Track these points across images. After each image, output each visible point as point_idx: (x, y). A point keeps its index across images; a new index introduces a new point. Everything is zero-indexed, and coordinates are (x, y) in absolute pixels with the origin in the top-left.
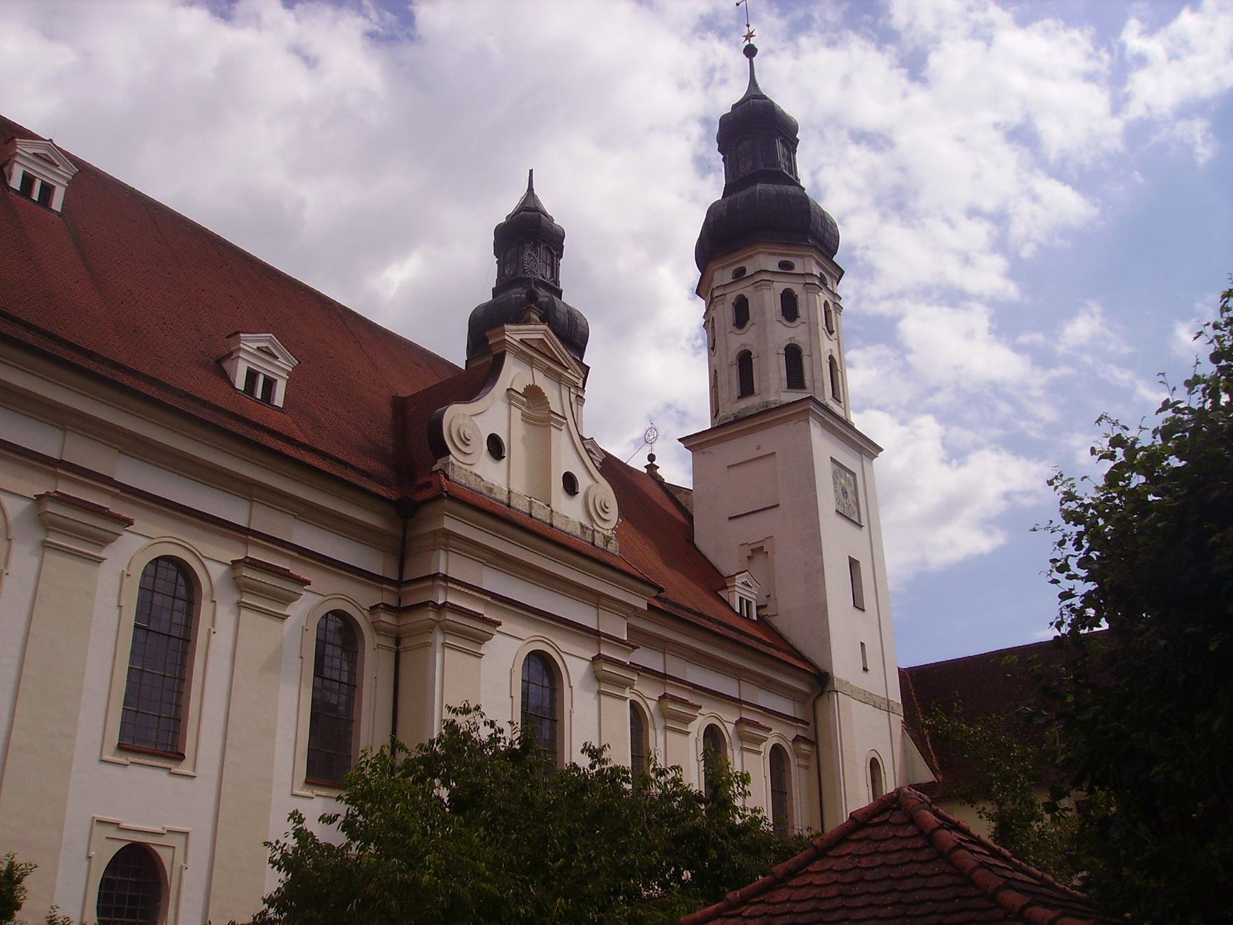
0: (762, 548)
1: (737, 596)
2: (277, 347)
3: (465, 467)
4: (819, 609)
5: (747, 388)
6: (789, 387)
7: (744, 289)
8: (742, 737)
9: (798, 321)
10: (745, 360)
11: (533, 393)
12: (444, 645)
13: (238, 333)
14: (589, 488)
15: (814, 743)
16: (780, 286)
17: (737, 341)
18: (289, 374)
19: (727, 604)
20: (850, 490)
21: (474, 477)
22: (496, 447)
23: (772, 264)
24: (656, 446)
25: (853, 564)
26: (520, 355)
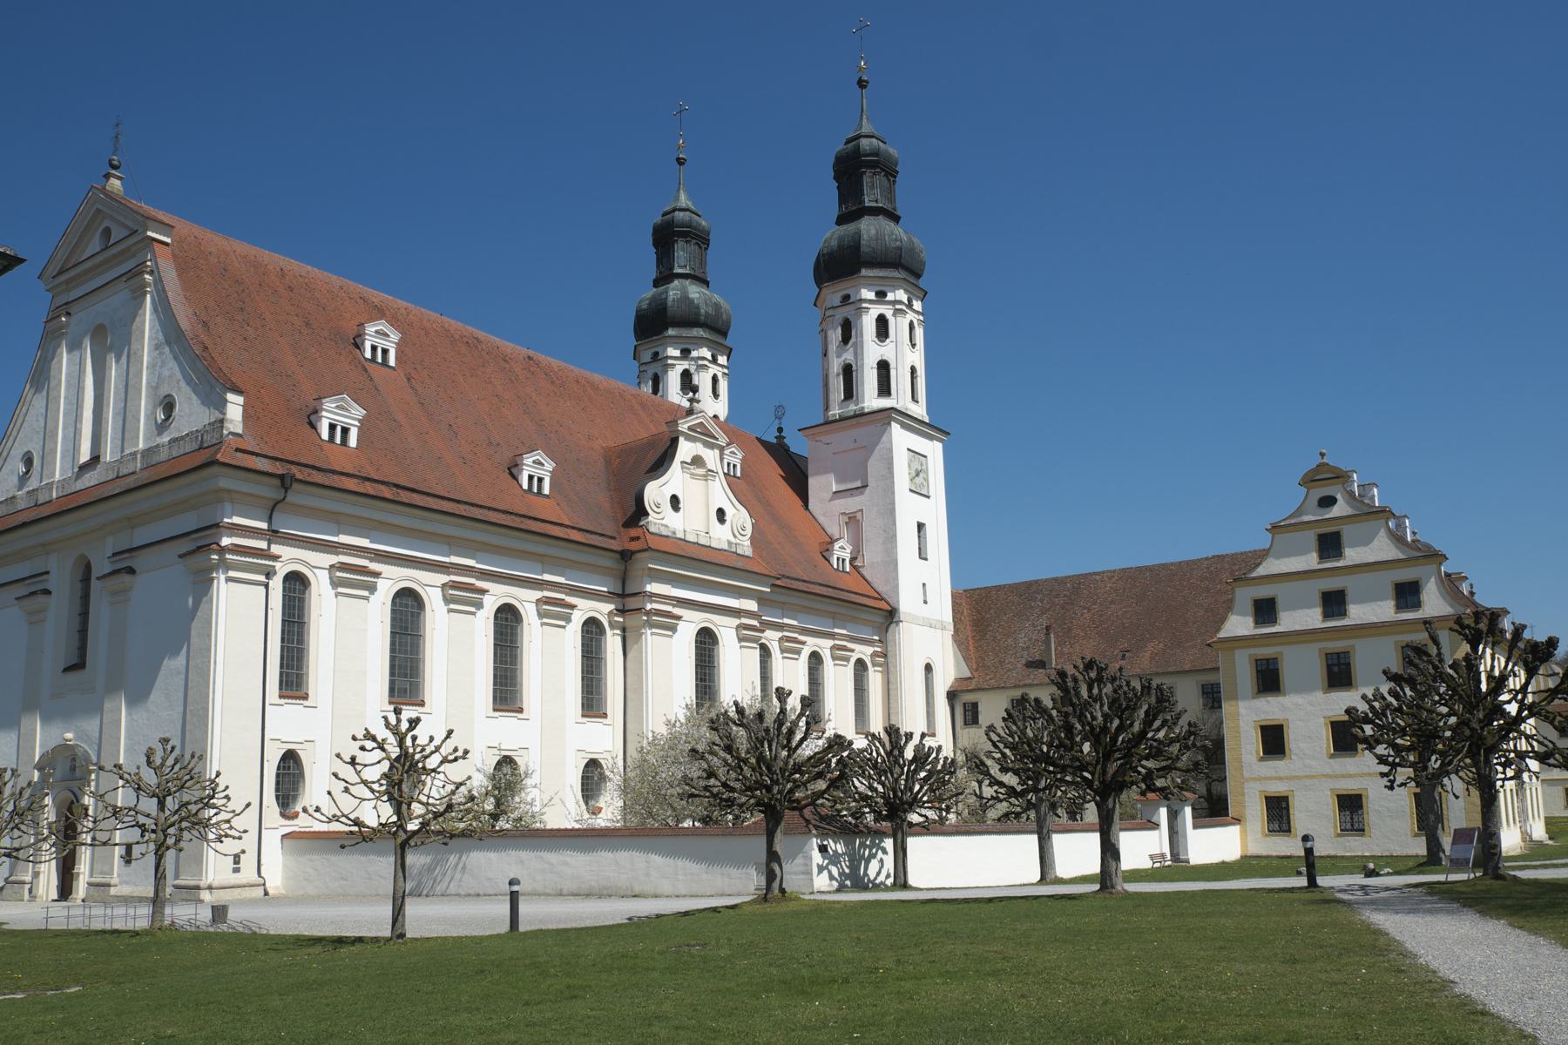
1: (835, 557)
3: (658, 521)
4: (892, 564)
6: (879, 396)
8: (834, 658)
11: (697, 461)
12: (652, 634)
13: (522, 455)
14: (734, 515)
15: (885, 656)
22: (675, 502)
24: (783, 421)
25: (920, 526)
26: (689, 438)
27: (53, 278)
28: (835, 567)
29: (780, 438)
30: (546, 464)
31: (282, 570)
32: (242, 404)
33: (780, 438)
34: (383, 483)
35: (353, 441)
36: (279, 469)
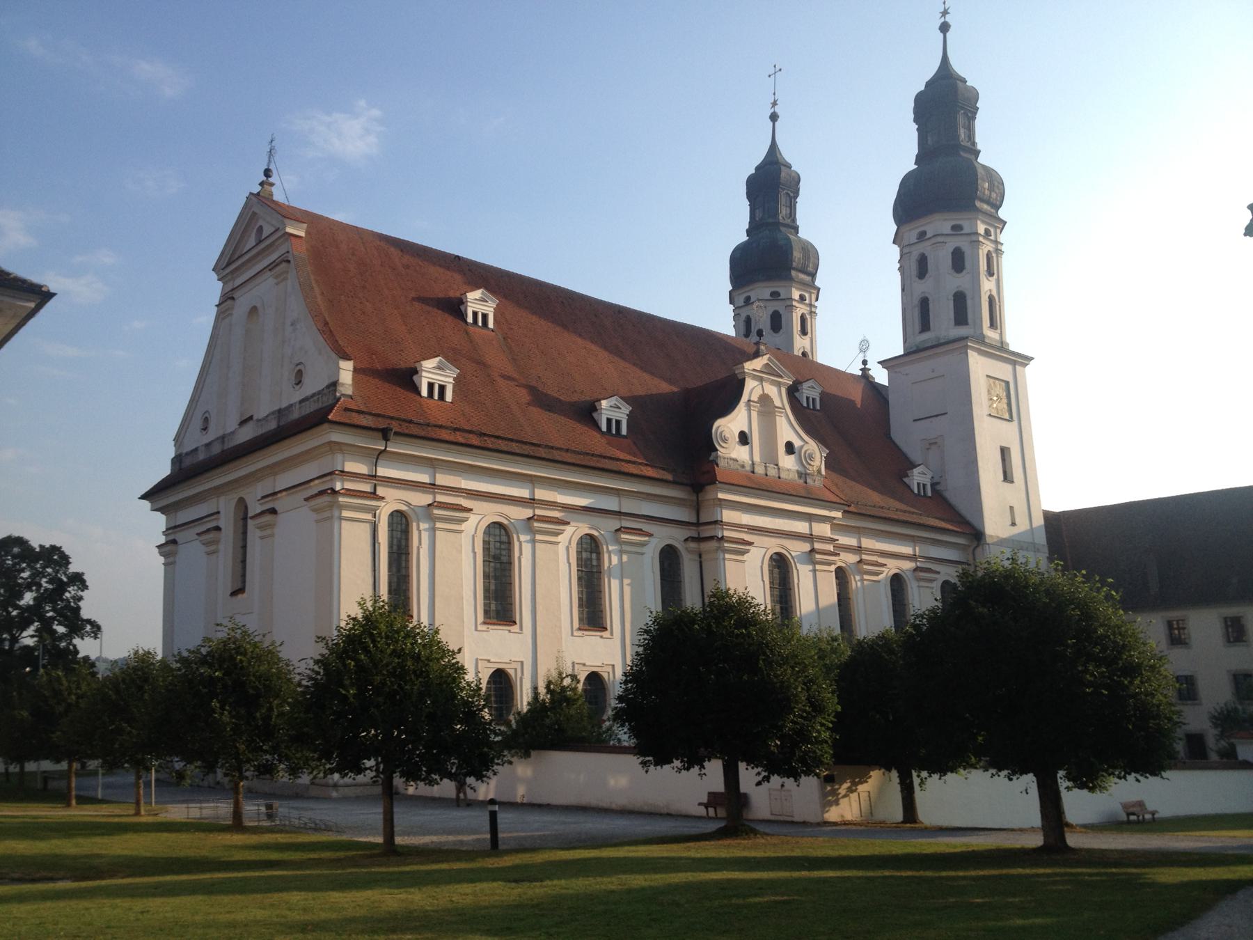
0: (936, 443)
2: (622, 404)
5: (925, 326)
7: (925, 247)
9: (964, 272)
10: (924, 304)
16: (952, 244)
17: (921, 288)
18: (627, 415)
19: (909, 487)
21: (732, 461)
23: (946, 228)
24: (867, 353)
26: (755, 378)
27: (223, 269)
28: (916, 491)
29: (865, 370)
30: (623, 408)
31: (385, 511)
32: (341, 371)
33: (865, 370)
34: (470, 432)
35: (449, 396)
36: (382, 424)
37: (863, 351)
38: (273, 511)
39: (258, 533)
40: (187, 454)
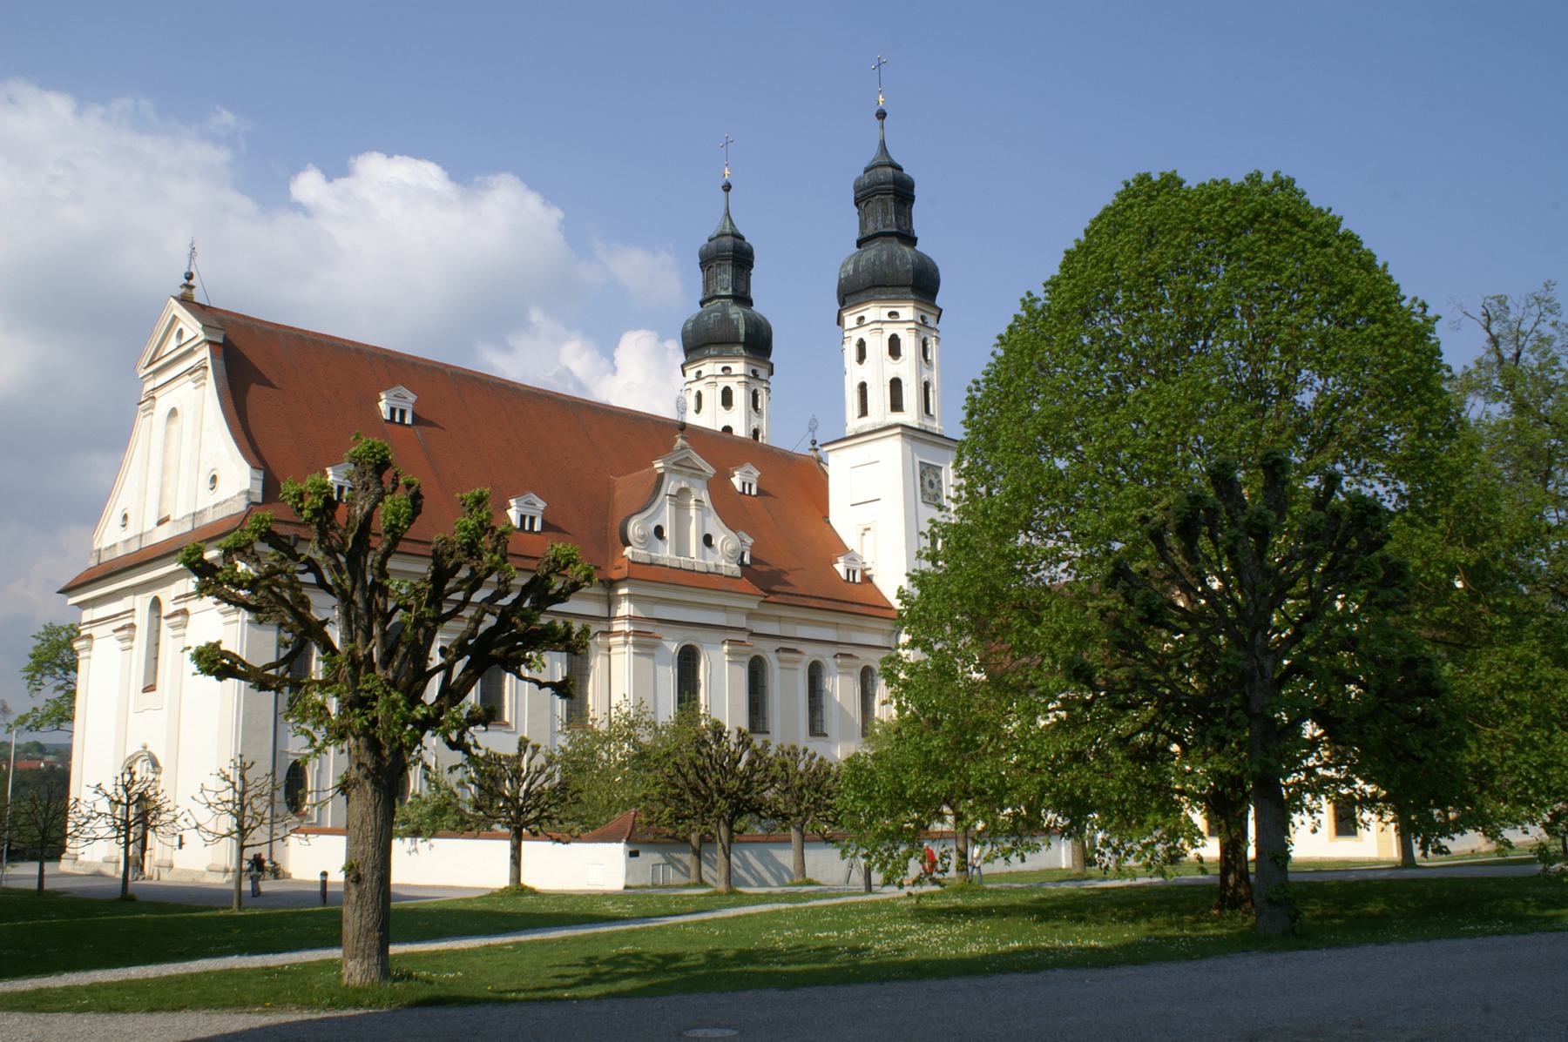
7: (863, 333)
16: (890, 330)
20: (935, 481)
37: (812, 430)
38: (185, 612)
39: (171, 632)
40: (106, 549)
